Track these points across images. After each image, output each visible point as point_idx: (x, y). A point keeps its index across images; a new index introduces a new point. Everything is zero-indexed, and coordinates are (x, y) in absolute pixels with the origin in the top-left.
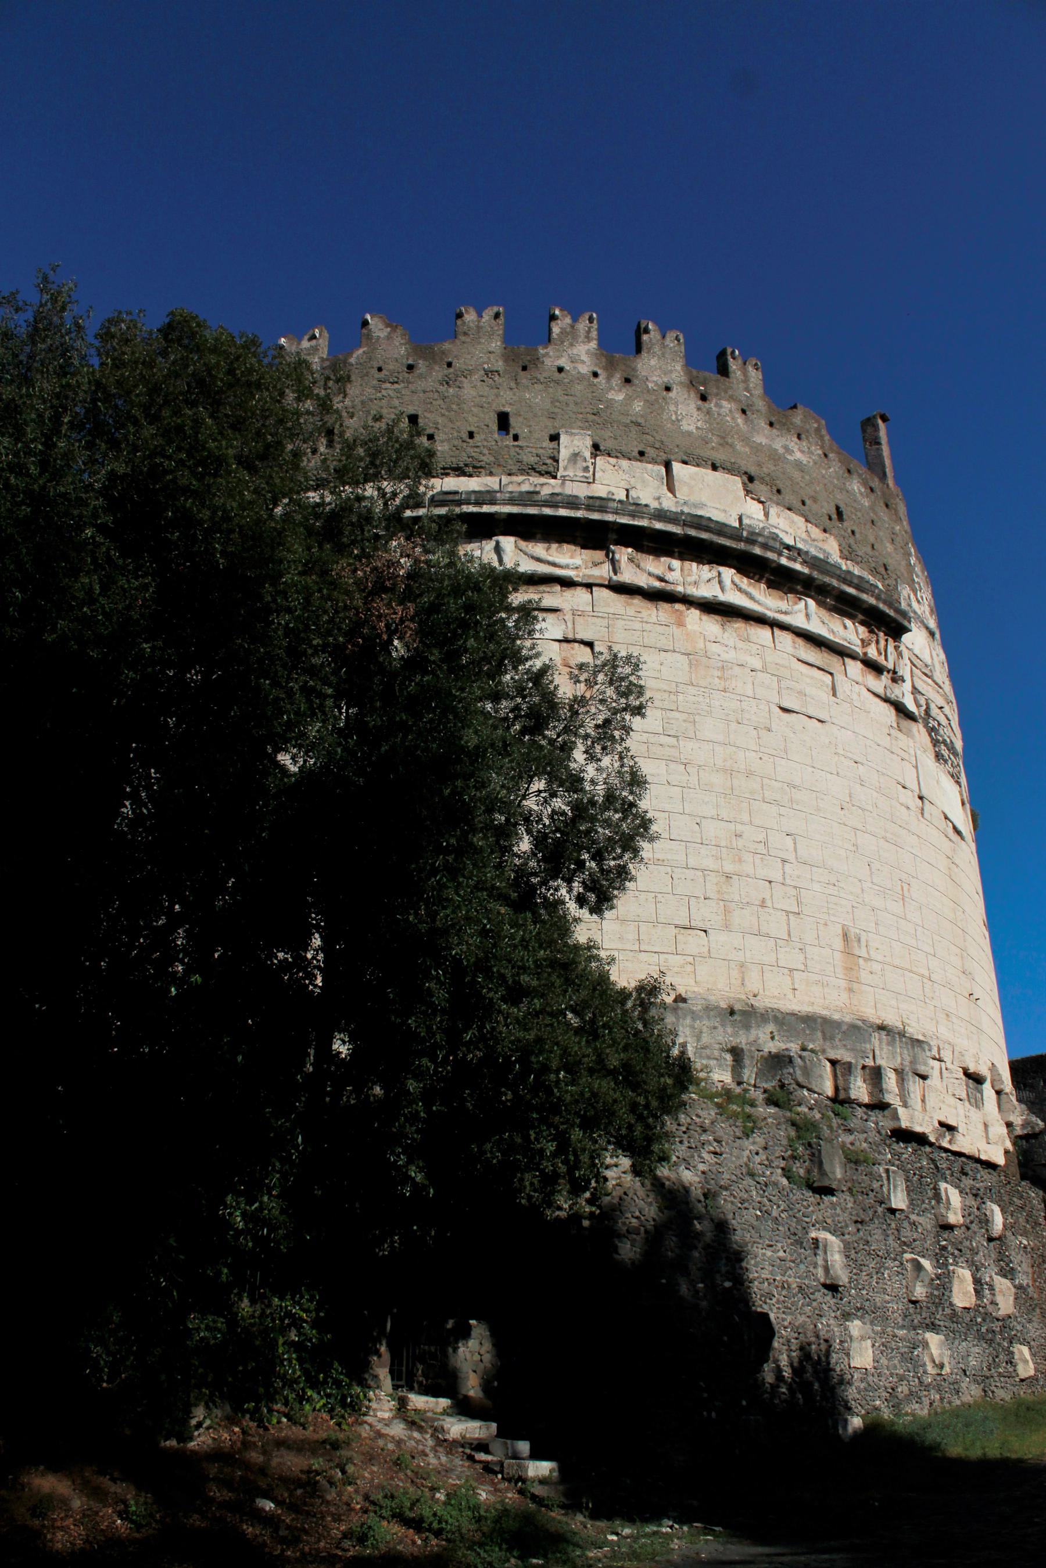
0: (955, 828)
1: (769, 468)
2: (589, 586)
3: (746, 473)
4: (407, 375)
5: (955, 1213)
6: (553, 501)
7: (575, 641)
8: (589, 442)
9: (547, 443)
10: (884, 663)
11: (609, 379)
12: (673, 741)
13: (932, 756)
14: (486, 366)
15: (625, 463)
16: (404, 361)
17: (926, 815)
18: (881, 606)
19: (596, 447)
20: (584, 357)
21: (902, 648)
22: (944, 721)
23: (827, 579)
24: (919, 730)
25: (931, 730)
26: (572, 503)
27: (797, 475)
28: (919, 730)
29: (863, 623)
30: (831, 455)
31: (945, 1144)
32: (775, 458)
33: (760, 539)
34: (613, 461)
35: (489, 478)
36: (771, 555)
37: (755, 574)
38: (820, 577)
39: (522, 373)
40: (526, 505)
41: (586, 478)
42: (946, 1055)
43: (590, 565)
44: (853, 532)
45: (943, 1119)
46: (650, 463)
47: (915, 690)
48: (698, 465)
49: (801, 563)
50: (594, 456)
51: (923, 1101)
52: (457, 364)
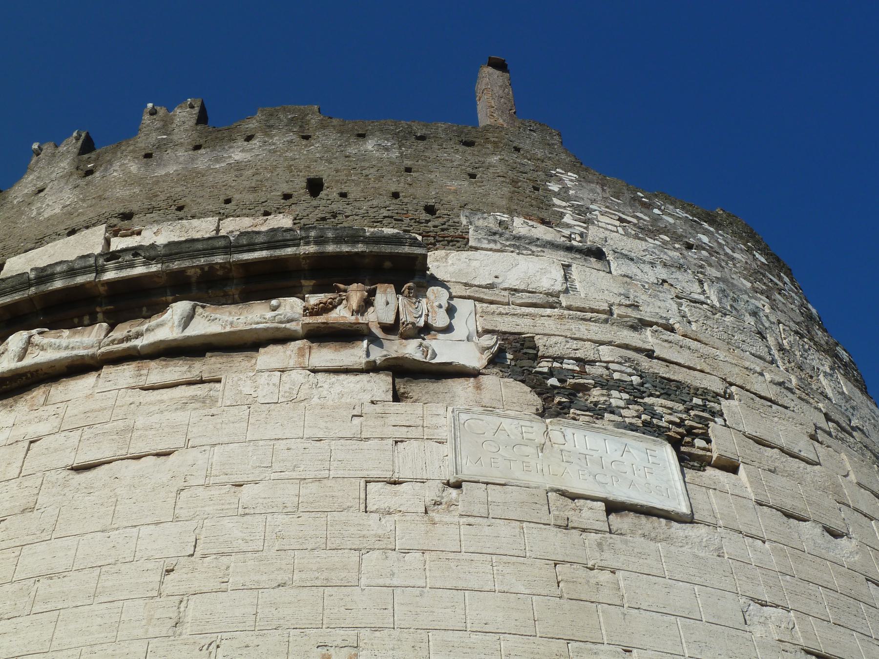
18: (331, 248)
23: (202, 261)
33: (58, 269)
36: (80, 280)
37: (81, 317)
38: (186, 264)
49: (145, 264)
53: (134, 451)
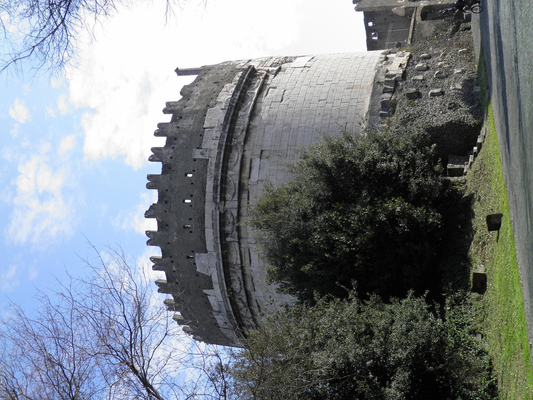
0: (312, 58)
1: (204, 101)
2: (244, 151)
3: (206, 107)
4: (169, 203)
5: (424, 65)
6: (218, 158)
7: (261, 155)
8: (197, 150)
9: (197, 162)
10: (265, 74)
11: (175, 144)
12: (292, 130)
13: (291, 63)
14: (168, 179)
15: (204, 140)
16: (164, 204)
17: (310, 66)
19: (198, 148)
20: (167, 151)
21: (258, 68)
22: (278, 60)
24: (284, 66)
25: (282, 63)
26: (219, 153)
27: (205, 94)
28: (284, 66)
29: (252, 78)
30: (197, 84)
31: (405, 67)
32: (200, 98)
34: (203, 143)
35: (207, 178)
36: (235, 101)
39: (172, 169)
40: (219, 167)
41: (209, 151)
42: (380, 65)
43: (237, 150)
44: (222, 79)
45: (398, 67)
46: (204, 134)
47: (271, 66)
48: (204, 120)
50: (201, 148)
51: (394, 71)
52: (166, 188)
53: (282, 94)
